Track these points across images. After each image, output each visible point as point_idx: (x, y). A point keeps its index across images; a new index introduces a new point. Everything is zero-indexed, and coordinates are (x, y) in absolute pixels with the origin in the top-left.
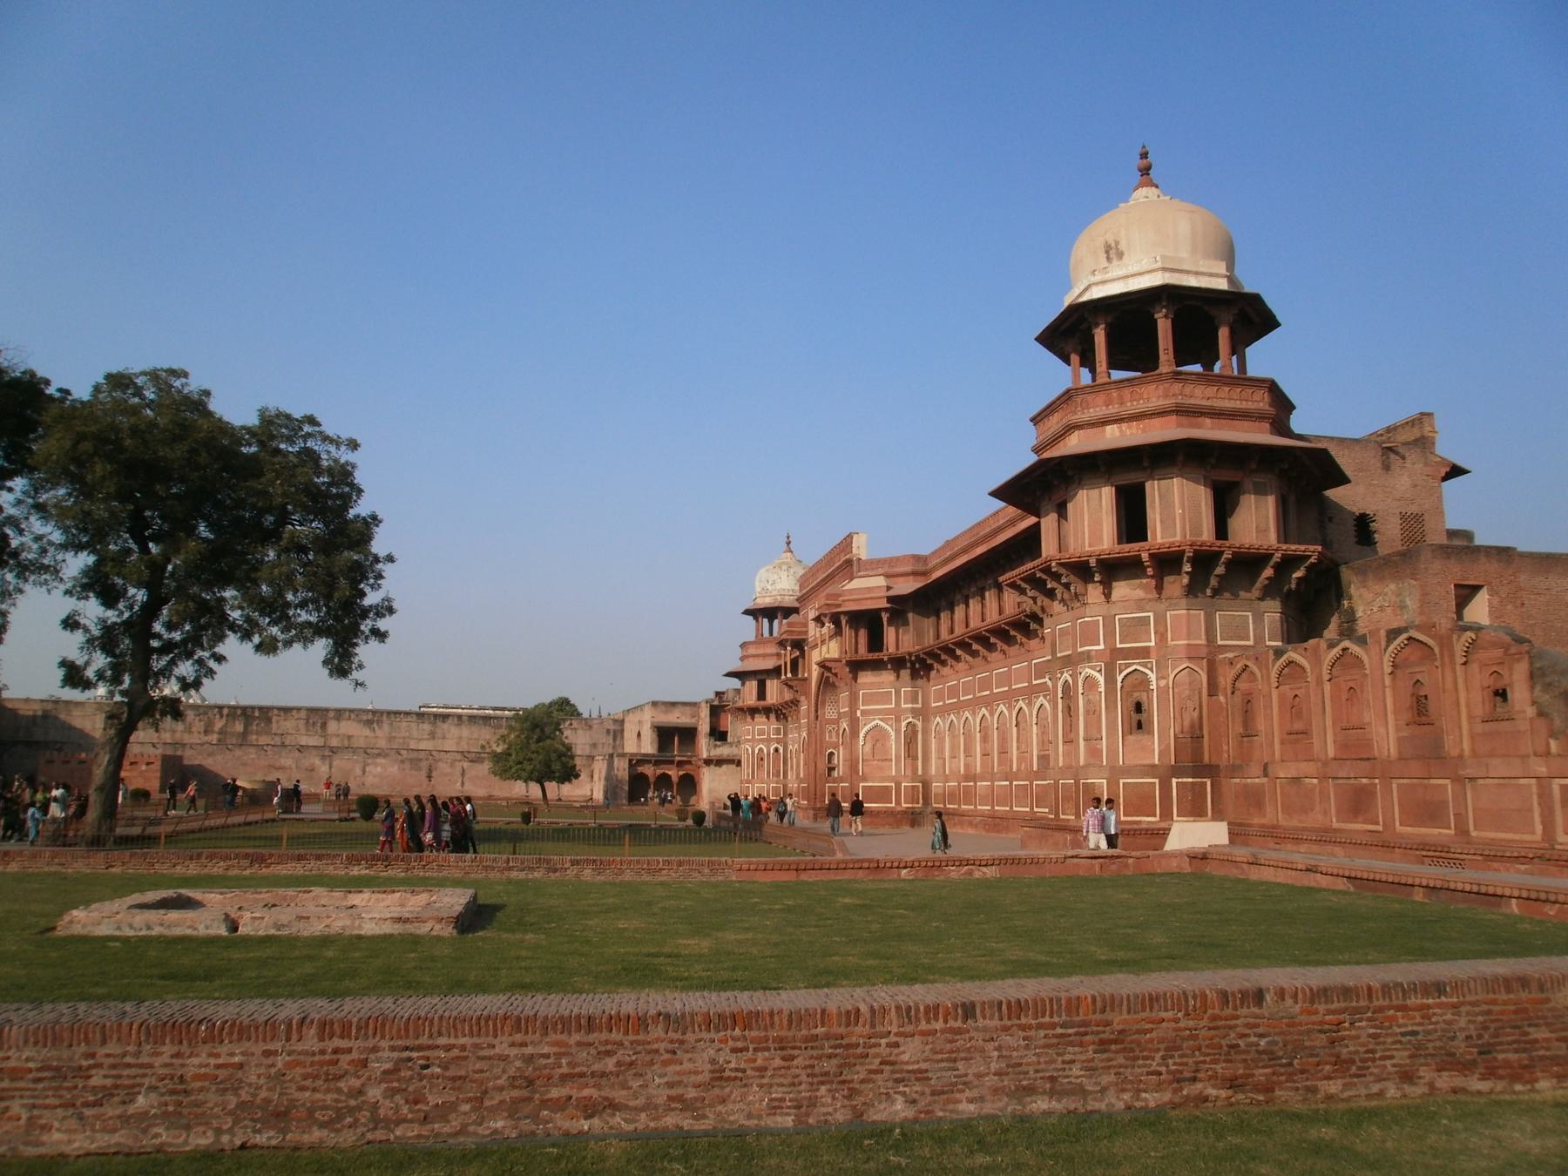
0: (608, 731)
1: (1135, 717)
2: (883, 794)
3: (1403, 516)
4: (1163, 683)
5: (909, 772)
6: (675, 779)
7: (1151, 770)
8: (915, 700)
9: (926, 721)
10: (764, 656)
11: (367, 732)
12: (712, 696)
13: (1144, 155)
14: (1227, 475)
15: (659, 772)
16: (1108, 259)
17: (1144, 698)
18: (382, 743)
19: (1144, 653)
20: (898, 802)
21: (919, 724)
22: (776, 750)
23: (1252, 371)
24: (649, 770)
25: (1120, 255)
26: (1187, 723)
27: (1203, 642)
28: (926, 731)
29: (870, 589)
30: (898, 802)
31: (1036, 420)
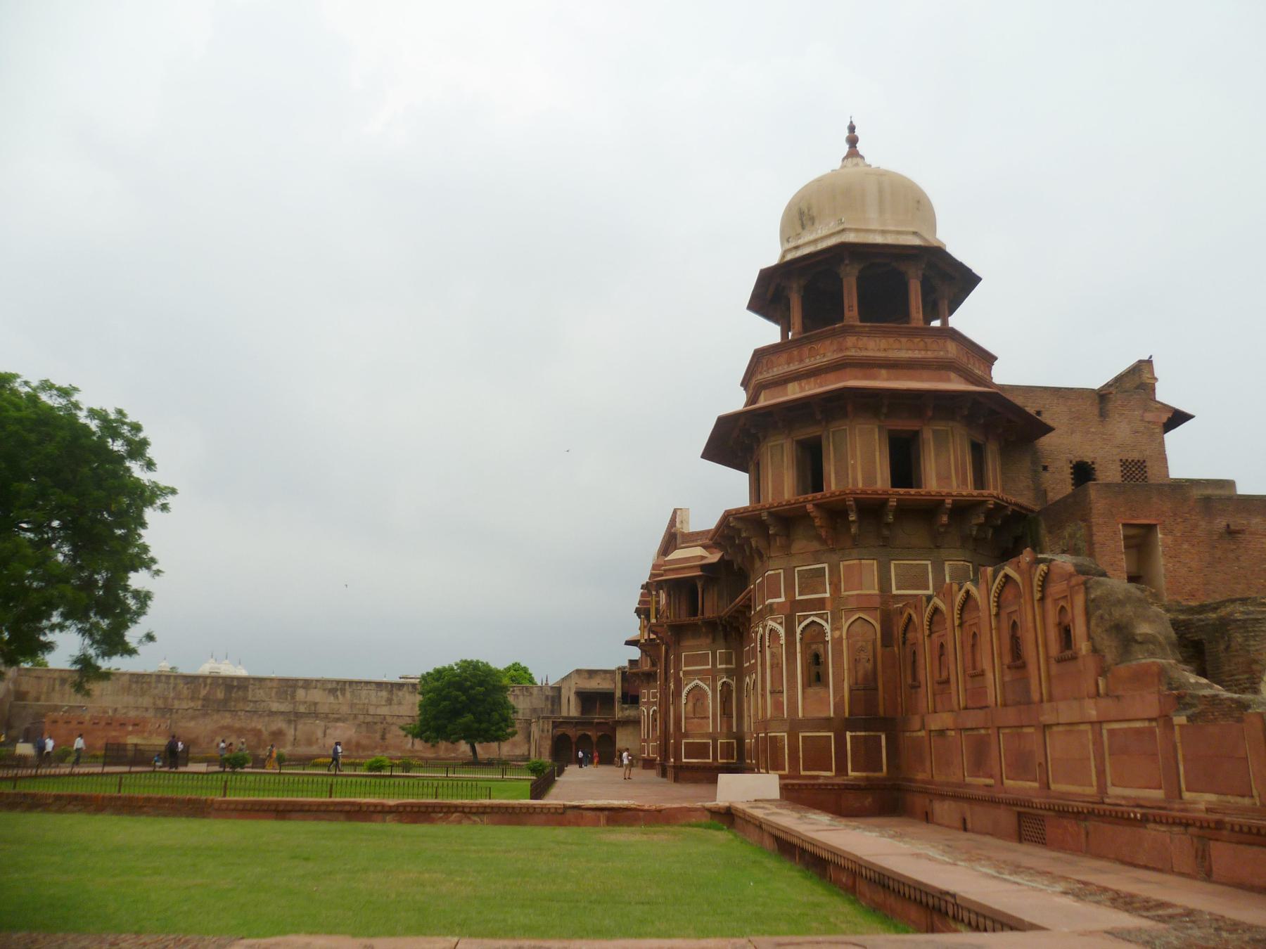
0: (547, 697)
3: (1124, 463)
4: (837, 634)
5: (725, 730)
6: (594, 739)
7: (826, 723)
8: (729, 662)
9: (740, 681)
11: (332, 699)
12: (626, 664)
13: (852, 128)
14: (904, 424)
15: (580, 733)
18: (345, 709)
19: (820, 604)
21: (734, 684)
24: (573, 733)
25: (812, 219)
26: (861, 673)
27: (876, 592)
28: (740, 690)
30: (715, 758)
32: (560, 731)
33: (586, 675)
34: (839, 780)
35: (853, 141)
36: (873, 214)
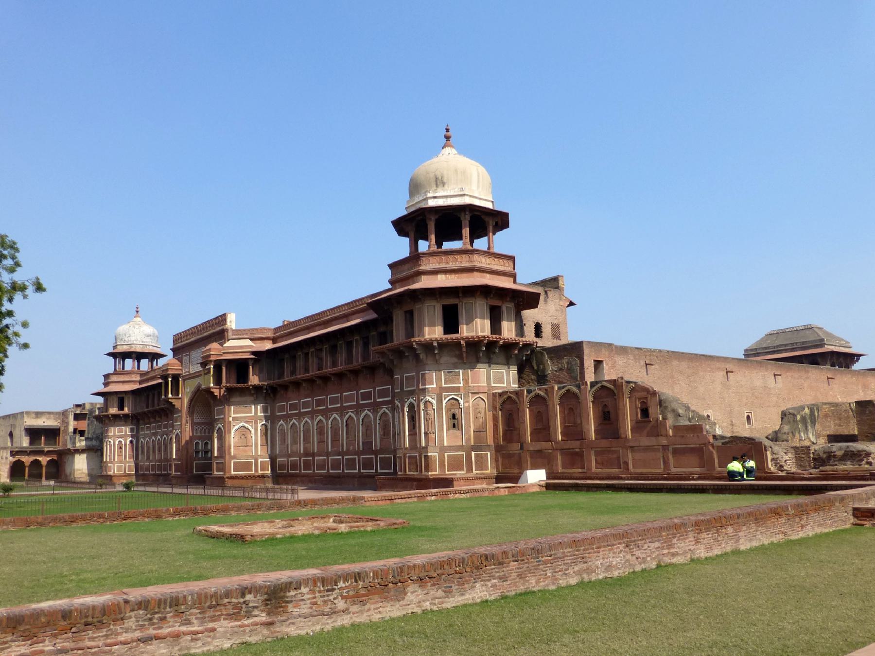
1: (452, 421)
2: (247, 466)
3: (553, 325)
4: (467, 405)
10: (124, 382)
14: (496, 303)
16: (437, 186)
17: (457, 412)
19: (458, 389)
20: (256, 470)
22: (131, 442)
23: (496, 249)
24: (27, 460)
25: (444, 184)
29: (241, 347)
30: (256, 470)
31: (391, 266)
32: (17, 458)
33: (34, 415)
34: (469, 475)
35: (448, 138)
36: (474, 187)
